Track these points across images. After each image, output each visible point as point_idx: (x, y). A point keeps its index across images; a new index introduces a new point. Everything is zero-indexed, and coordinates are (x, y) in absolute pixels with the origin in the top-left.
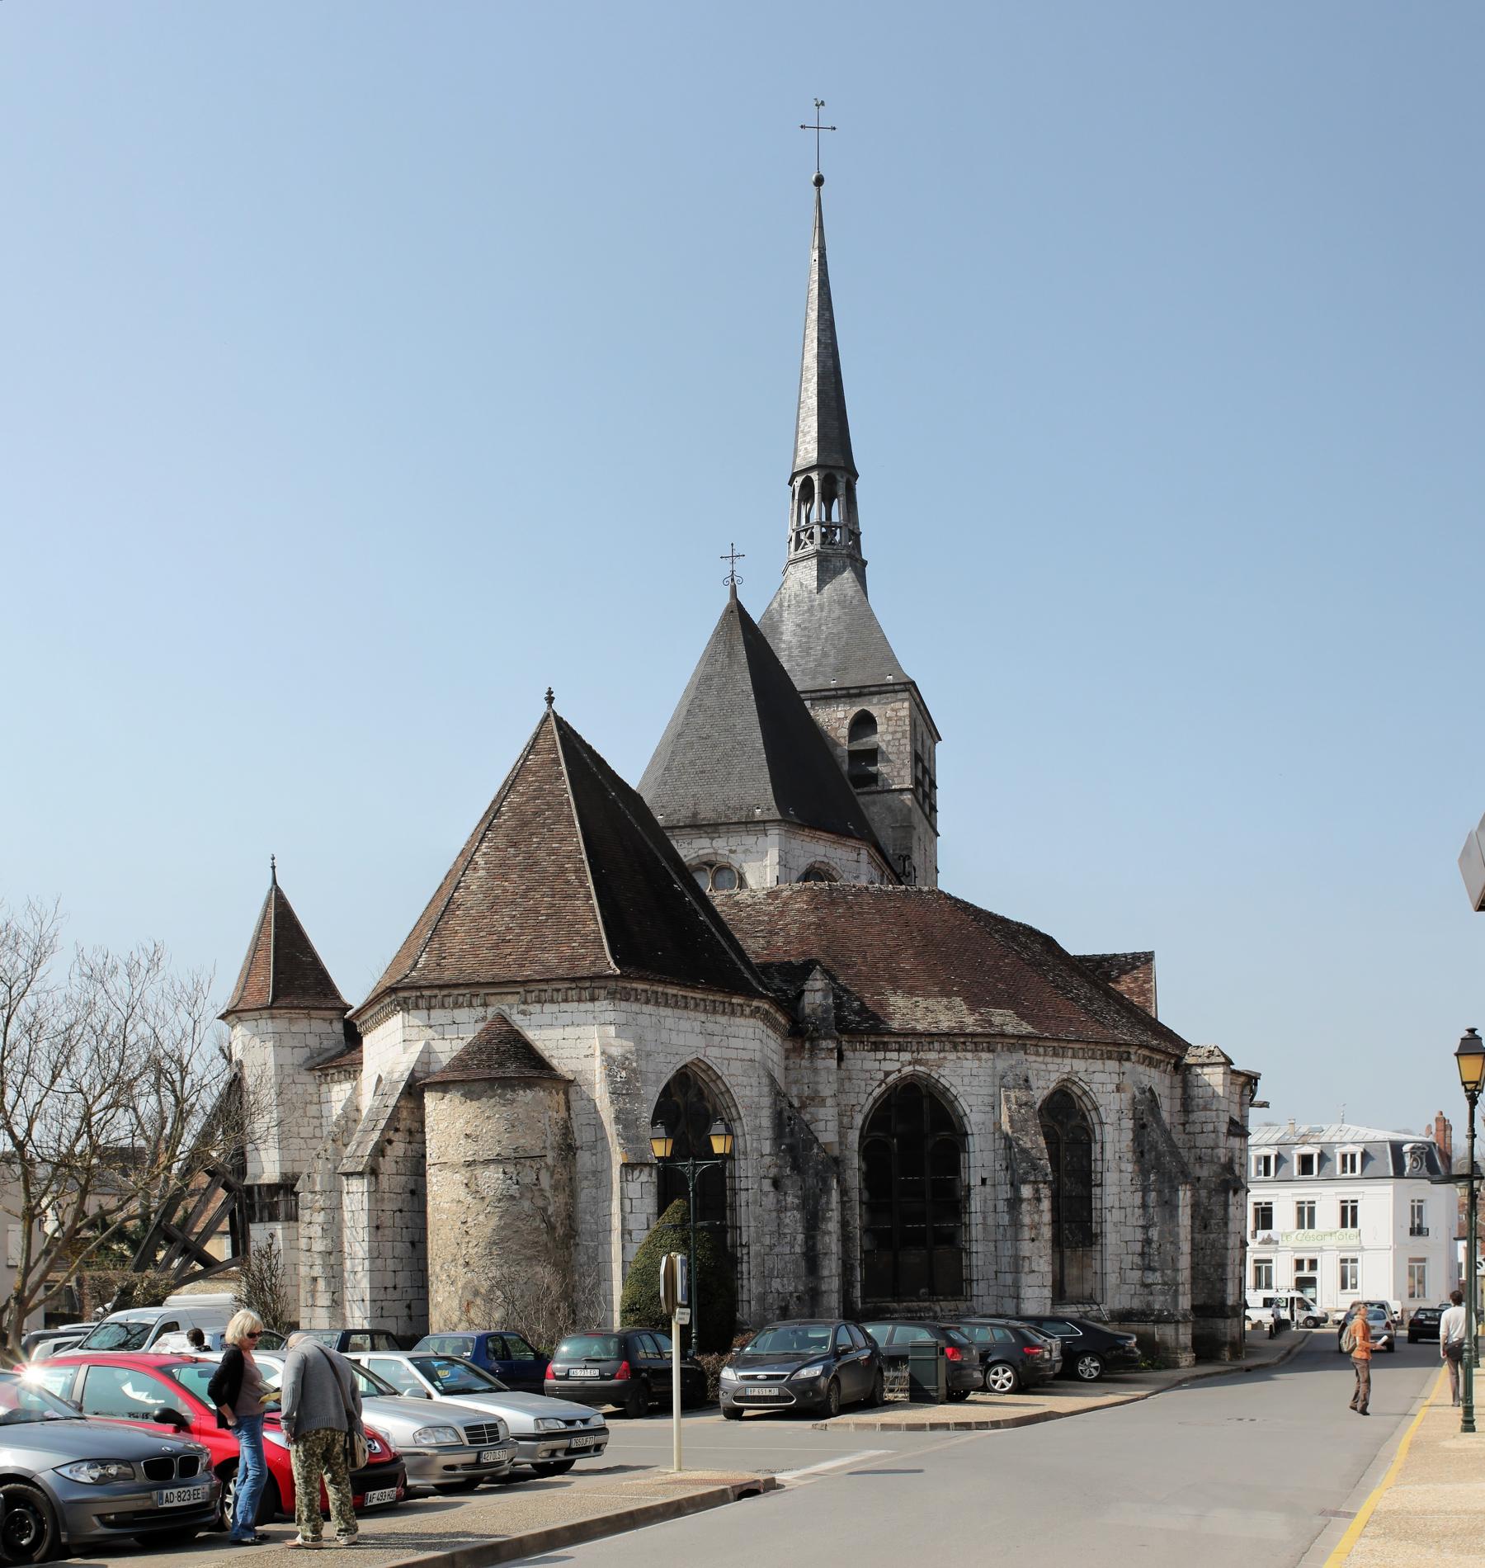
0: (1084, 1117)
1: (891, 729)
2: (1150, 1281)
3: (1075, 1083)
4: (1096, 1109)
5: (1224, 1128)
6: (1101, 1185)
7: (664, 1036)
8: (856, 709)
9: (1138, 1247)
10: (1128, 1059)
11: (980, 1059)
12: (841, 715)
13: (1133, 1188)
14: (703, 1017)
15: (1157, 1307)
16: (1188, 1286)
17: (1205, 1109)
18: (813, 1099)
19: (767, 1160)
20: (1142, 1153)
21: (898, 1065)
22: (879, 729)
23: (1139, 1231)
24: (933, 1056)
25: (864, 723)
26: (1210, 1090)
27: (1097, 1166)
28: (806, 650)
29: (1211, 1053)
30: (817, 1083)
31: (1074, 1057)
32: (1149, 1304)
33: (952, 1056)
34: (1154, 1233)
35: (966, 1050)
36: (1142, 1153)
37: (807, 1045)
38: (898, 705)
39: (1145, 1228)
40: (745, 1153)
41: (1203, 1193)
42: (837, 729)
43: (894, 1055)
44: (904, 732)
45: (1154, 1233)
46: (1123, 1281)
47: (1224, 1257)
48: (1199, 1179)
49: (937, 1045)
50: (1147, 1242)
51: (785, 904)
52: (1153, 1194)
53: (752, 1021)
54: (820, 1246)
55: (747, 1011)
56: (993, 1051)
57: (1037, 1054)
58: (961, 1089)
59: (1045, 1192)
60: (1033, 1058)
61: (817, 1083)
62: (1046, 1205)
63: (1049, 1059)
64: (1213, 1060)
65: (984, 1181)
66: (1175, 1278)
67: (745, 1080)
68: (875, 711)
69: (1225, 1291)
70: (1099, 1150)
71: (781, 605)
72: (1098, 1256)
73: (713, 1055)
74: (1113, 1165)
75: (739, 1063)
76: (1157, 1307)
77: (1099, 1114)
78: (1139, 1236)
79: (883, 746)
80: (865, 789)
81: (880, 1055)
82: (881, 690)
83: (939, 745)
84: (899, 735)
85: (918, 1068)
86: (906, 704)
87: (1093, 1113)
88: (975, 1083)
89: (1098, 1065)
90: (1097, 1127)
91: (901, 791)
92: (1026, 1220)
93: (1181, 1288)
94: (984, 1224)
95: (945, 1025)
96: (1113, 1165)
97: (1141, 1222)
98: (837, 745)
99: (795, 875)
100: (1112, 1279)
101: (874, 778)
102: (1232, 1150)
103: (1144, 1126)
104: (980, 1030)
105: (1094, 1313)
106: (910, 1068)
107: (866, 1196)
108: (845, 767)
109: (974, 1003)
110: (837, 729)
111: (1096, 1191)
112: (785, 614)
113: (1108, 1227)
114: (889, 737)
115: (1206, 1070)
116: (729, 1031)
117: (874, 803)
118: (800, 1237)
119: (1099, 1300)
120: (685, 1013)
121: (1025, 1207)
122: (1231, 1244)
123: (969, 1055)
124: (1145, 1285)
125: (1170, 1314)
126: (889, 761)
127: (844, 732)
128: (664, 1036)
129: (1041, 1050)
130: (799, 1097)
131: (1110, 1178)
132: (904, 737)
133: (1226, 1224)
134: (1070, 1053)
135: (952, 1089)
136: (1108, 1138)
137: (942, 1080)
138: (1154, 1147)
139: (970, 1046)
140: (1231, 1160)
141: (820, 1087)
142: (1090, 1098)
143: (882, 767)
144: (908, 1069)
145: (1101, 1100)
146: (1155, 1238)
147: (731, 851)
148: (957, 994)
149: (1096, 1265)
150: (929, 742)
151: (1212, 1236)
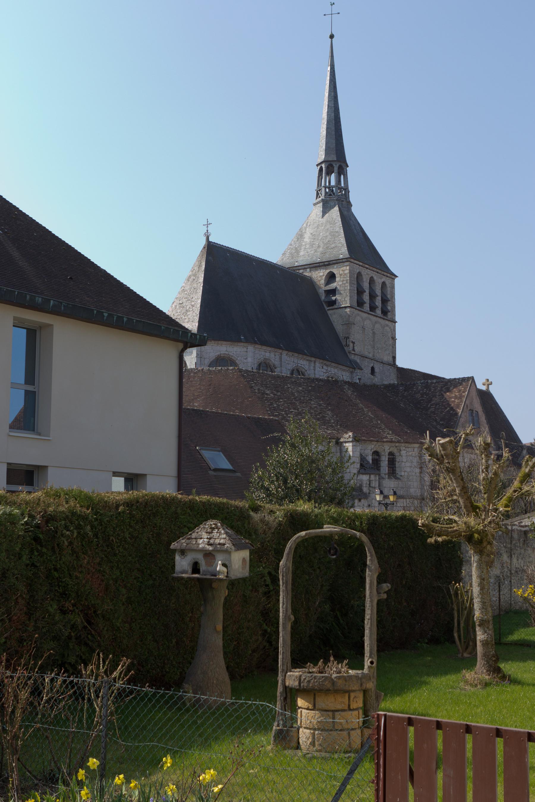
1: (342, 279)
8: (328, 271)
12: (321, 274)
22: (337, 279)
25: (331, 277)
28: (312, 245)
38: (344, 268)
42: (320, 281)
44: (347, 280)
68: (335, 271)
79: (338, 287)
83: (396, 280)
86: (348, 268)
91: (345, 307)
98: (320, 288)
99: (207, 362)
101: (334, 302)
108: (323, 297)
110: (320, 281)
112: (307, 229)
114: (340, 283)
126: (341, 294)
127: (323, 282)
132: (347, 283)
143: (338, 297)
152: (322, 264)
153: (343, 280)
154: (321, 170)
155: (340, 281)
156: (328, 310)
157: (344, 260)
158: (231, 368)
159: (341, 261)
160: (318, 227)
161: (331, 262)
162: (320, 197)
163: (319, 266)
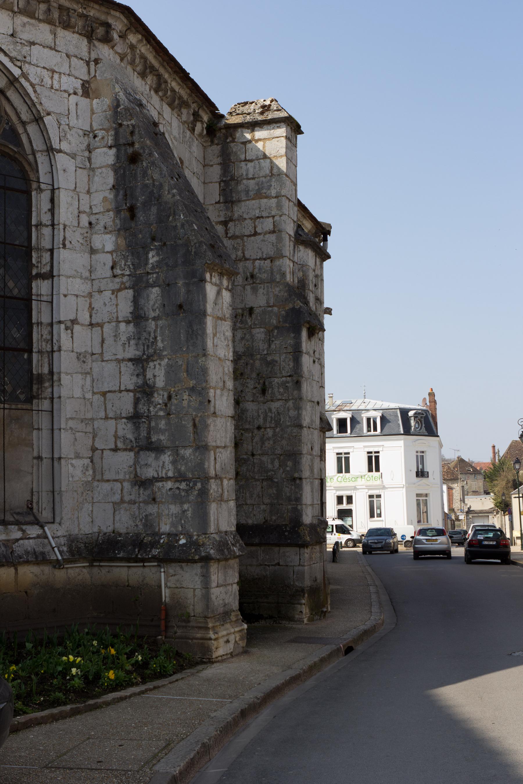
0: (13, 135)
2: (150, 473)
4: (38, 120)
6: (50, 276)
9: (125, 404)
10: (107, 39)
13: (116, 284)
15: (165, 528)
16: (229, 485)
17: (259, 195)
20: (132, 210)
23: (128, 369)
26: (266, 164)
27: (42, 238)
29: (266, 108)
32: (148, 522)
34: (158, 374)
36: (132, 210)
39: (140, 362)
41: (259, 333)
45: (158, 374)
46: (99, 476)
47: (297, 440)
48: (251, 310)
50: (145, 391)
52: (156, 291)
64: (270, 116)
66: (201, 465)
69: (299, 500)
70: (46, 206)
72: (44, 421)
74: (75, 237)
76: (165, 528)
77: (44, 131)
78: (129, 380)
87: (32, 129)
89: (42, 32)
90: (41, 159)
93: (213, 486)
96: (75, 237)
97: (132, 352)
100: (74, 471)
103: (134, 159)
105: (29, 544)
111: (40, 287)
113: (65, 362)
115: (259, 134)
119: (45, 515)
124: (142, 483)
125: (192, 544)
131: (70, 261)
133: (298, 384)
138: (154, 197)
142: (24, 95)
145: (48, 102)
146: (160, 382)
149: (41, 442)
151: (275, 405)
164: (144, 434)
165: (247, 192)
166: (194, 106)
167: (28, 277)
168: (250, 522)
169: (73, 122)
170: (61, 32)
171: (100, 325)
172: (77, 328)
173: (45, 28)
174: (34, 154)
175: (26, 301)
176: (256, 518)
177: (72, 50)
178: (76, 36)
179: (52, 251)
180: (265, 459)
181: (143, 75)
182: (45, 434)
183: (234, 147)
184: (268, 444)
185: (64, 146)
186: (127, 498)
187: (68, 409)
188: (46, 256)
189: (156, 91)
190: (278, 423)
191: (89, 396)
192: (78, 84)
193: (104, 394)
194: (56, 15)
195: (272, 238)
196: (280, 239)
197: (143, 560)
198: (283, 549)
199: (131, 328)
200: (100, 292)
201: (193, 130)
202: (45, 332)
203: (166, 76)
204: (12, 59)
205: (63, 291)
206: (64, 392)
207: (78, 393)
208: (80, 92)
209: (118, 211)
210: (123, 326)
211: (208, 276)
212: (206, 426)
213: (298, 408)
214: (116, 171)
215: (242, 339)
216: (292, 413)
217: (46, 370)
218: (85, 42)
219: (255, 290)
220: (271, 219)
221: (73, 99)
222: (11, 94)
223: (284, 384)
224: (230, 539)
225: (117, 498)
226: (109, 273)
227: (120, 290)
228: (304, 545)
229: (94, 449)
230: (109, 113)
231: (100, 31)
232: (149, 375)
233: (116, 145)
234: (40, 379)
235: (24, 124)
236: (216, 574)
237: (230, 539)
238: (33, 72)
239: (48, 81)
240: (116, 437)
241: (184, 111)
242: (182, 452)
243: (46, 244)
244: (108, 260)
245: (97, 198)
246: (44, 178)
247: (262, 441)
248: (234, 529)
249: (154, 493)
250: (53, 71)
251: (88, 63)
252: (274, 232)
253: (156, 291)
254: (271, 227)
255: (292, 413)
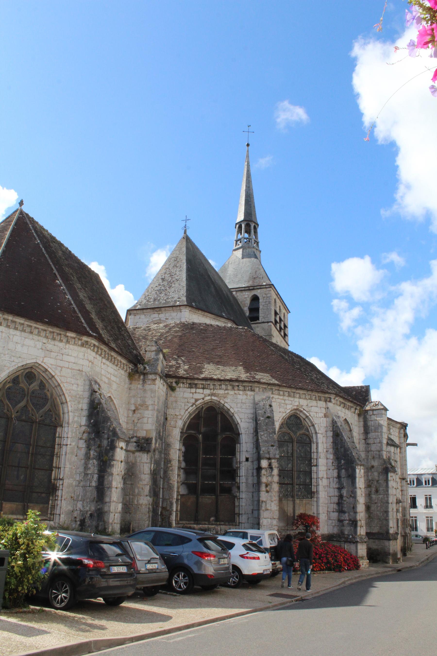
1: (264, 301)
2: (343, 518)
3: (301, 411)
4: (313, 425)
5: (385, 441)
6: (316, 466)
7: (11, 346)
9: (336, 500)
10: (330, 401)
11: (247, 395)
13: (333, 468)
14: (45, 340)
17: (375, 431)
18: (142, 406)
19: (83, 428)
21: (202, 396)
23: (336, 490)
24: (221, 392)
26: (377, 422)
27: (314, 456)
28: (236, 275)
30: (145, 397)
31: (300, 398)
33: (232, 392)
35: (239, 390)
37: (142, 377)
40: (68, 423)
43: (201, 391)
45: (344, 492)
47: (387, 507)
49: (223, 386)
50: (341, 497)
51: (170, 329)
52: (343, 470)
53: (83, 349)
54: (106, 482)
55: (80, 342)
56: (254, 391)
57: (279, 395)
58: (236, 410)
59: (275, 464)
60: (277, 397)
61: (145, 397)
62: (276, 472)
63: (286, 398)
65: (247, 460)
67: (73, 381)
69: (388, 525)
71: (229, 263)
72: (315, 504)
73: (49, 363)
75: (69, 371)
78: (337, 494)
80: (255, 322)
81: (193, 390)
82: (261, 287)
84: (267, 303)
85: (213, 398)
87: (312, 428)
88: (244, 407)
89: (314, 403)
92: (264, 480)
93: (359, 523)
94: (247, 483)
95: (228, 378)
97: (337, 486)
102: (390, 452)
104: (247, 379)
106: (209, 398)
107: (183, 465)
109: (248, 369)
111: (314, 469)
112: (230, 266)
113: (321, 488)
114: (264, 304)
116: (64, 351)
117: (258, 327)
118: (96, 476)
120: (31, 336)
121: (263, 472)
122: (390, 500)
123: (241, 392)
128: (11, 346)
129: (281, 393)
130: (135, 404)
133: (388, 491)
134: (298, 396)
135: (231, 410)
136: (320, 441)
137: (226, 405)
139: (241, 388)
140: (389, 459)
141: (147, 400)
142: (310, 420)
144: (208, 398)
145: (316, 421)
146: (345, 495)
147: (166, 319)
148: (241, 366)
150: (283, 311)
151: (381, 496)
152: (248, 288)
153: (266, 302)
154: (240, 227)
155: (263, 302)
156: (252, 324)
157: (267, 286)
158: (241, 327)
159: (265, 286)
160: (239, 264)
161: (256, 288)
162: (239, 245)
163: (244, 290)
164: (341, 508)
165: (372, 430)
166: (355, 407)
167: (310, 465)
168: (374, 532)
169: (322, 425)
170: (318, 402)
171: (329, 478)
172: (323, 479)
173: (315, 402)
174: (312, 434)
175: (310, 473)
176: (376, 530)
177: (321, 406)
178: (322, 402)
179: (317, 459)
180: (378, 513)
181: (340, 405)
182: (315, 507)
183: (368, 417)
184: (379, 508)
185: (320, 432)
186: (336, 525)
187: (321, 501)
188: (315, 461)
189: (344, 408)
190: (382, 502)
191: (326, 497)
192: (323, 415)
193: (330, 497)
194: (317, 398)
195: (379, 445)
196: (382, 445)
197: (341, 541)
198: (384, 541)
199: (337, 480)
200: (329, 469)
201: (355, 413)
202: (315, 480)
203: (346, 403)
204: (307, 412)
205: (320, 469)
206: (320, 496)
207: (323, 496)
208: (324, 416)
209: (333, 448)
210: (335, 479)
211: (357, 467)
212: (356, 507)
213: (388, 497)
214: (333, 438)
215: (371, 475)
216: (386, 499)
217: (315, 490)
218: (325, 403)
219: (374, 461)
220: (378, 439)
221: (322, 418)
222: (306, 419)
223: (383, 490)
224: (364, 537)
225: (334, 524)
226: (331, 465)
227: (334, 469)
228: (390, 540)
229: (328, 511)
230: (331, 422)
231: (328, 399)
232: (342, 492)
233: (333, 431)
234: (314, 492)
235: (310, 426)
236: (360, 546)
237: (364, 537)
238: (312, 414)
239: (315, 415)
240: (334, 508)
241: (352, 409)
242: (351, 513)
243: (315, 457)
244: (331, 461)
245: (328, 445)
246: (315, 440)
247: (377, 507)
248: (365, 534)
249: (343, 524)
250: (317, 413)
251: (325, 409)
252: (380, 443)
253: (343, 470)
254: (379, 442)
255: (386, 499)
